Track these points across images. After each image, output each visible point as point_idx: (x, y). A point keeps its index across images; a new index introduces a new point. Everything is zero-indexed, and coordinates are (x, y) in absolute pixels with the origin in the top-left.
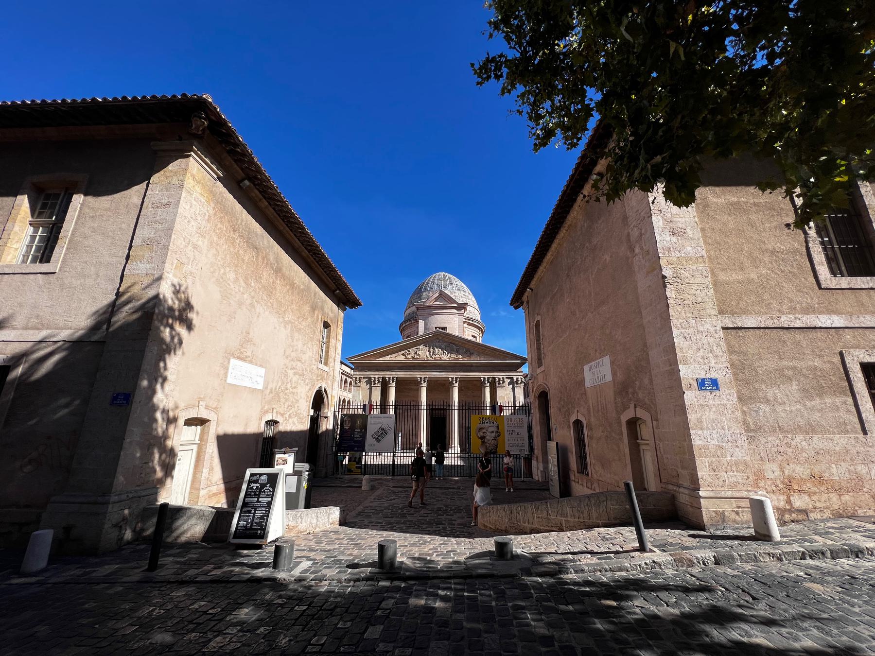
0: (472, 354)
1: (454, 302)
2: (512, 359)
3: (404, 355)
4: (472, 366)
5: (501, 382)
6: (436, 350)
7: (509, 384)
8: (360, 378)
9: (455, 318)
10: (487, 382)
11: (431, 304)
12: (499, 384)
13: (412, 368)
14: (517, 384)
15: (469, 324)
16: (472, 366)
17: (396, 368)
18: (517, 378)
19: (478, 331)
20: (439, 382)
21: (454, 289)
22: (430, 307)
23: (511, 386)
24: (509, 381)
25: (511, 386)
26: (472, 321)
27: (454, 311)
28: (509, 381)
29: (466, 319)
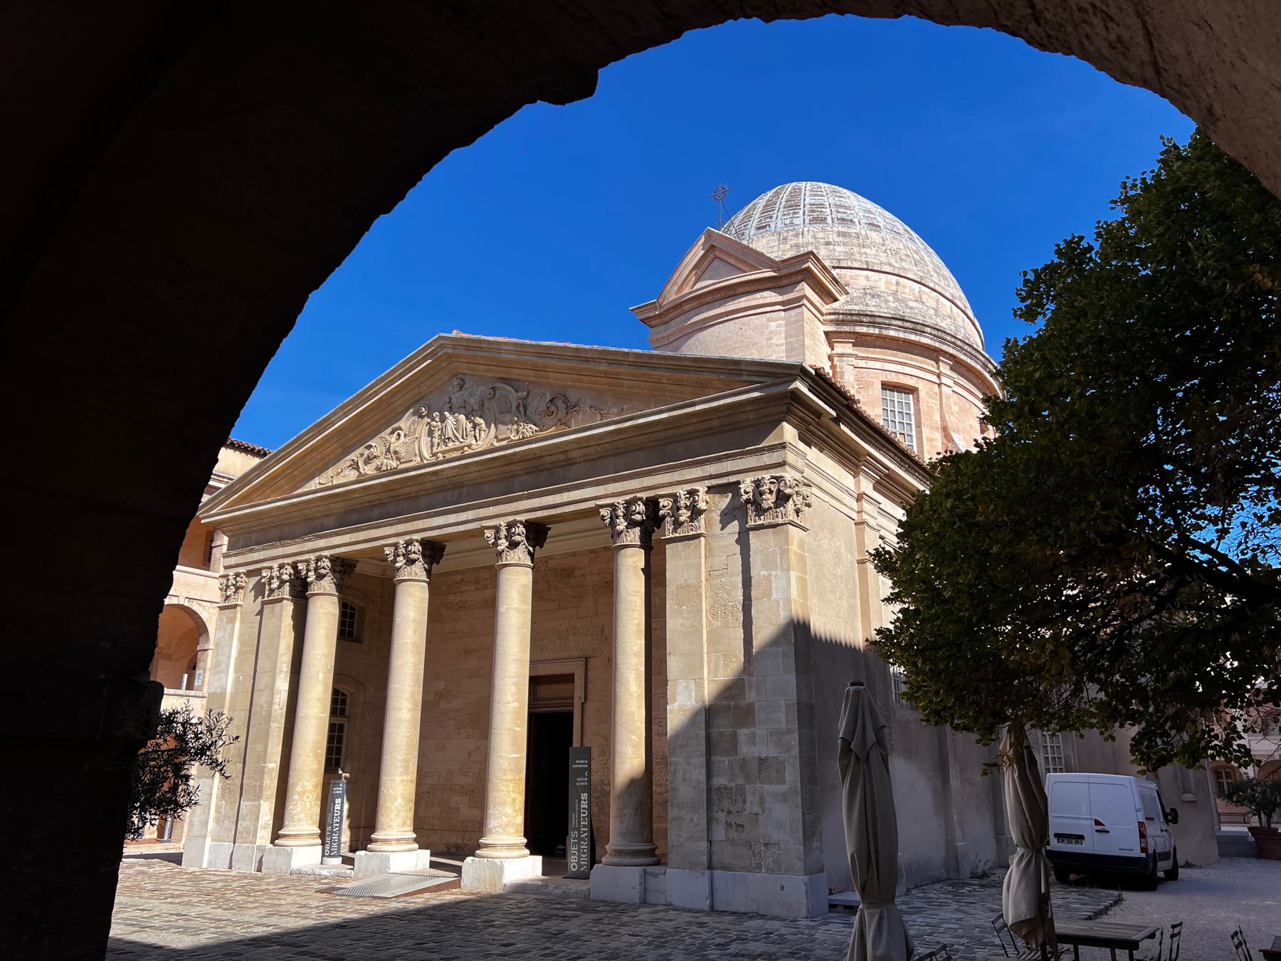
0: (571, 408)
1: (761, 260)
2: (702, 388)
3: (355, 466)
4: (570, 463)
5: (684, 515)
6: (451, 420)
7: (726, 517)
8: (237, 575)
9: (773, 325)
10: (622, 524)
11: (687, 290)
12: (677, 524)
13: (376, 512)
14: (760, 511)
15: (861, 341)
16: (570, 463)
17: (331, 521)
18: (758, 483)
19: (929, 364)
20: (551, 564)
21: (798, 221)
22: (680, 307)
23: (734, 526)
24: (724, 501)
25: (734, 526)
26: (873, 324)
27: (770, 296)
28: (724, 501)
29: (837, 322)
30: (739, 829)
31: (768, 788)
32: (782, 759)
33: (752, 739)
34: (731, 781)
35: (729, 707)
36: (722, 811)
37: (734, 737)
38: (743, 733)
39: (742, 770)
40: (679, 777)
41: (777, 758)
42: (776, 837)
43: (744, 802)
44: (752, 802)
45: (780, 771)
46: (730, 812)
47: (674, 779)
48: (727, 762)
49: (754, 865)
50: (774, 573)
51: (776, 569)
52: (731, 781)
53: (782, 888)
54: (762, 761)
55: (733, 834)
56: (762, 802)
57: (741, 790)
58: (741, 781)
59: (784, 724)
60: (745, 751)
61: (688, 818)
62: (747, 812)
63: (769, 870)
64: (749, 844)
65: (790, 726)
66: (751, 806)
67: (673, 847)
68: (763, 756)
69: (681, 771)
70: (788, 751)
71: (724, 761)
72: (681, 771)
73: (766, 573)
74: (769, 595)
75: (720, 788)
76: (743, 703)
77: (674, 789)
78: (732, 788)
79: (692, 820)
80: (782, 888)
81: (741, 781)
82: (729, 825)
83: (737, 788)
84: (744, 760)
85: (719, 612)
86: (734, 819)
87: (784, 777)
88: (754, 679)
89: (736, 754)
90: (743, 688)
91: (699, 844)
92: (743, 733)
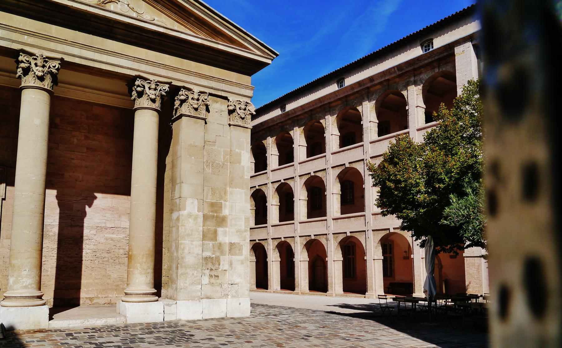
30: (217, 278)
31: (234, 258)
32: (242, 244)
33: (225, 233)
34: (213, 254)
35: (214, 216)
36: (208, 269)
37: (215, 232)
38: (220, 230)
39: (219, 249)
40: (186, 251)
41: (239, 243)
42: (237, 280)
43: (219, 265)
44: (223, 264)
45: (240, 249)
46: (211, 270)
47: (183, 253)
48: (211, 244)
49: (223, 295)
50: (243, 152)
51: (244, 150)
52: (213, 254)
53: (240, 304)
54: (231, 244)
55: (213, 280)
56: (231, 264)
57: (218, 260)
58: (218, 254)
59: (244, 227)
60: (221, 239)
61: (191, 273)
62: (220, 269)
63: (233, 297)
64: (221, 285)
65: (246, 229)
66: (224, 265)
67: (181, 289)
68: (233, 242)
69: (187, 249)
70: (245, 240)
71: (210, 244)
72: (187, 249)
73: (239, 151)
74: (240, 163)
75: (206, 257)
76: (221, 215)
77: (183, 258)
78: (213, 257)
79: (193, 274)
80: (240, 304)
81: (218, 254)
82: (211, 276)
83: (215, 258)
84: (220, 244)
85: (210, 165)
86: (213, 273)
87: (242, 252)
88: (227, 203)
89: (216, 240)
90: (221, 207)
91: (197, 286)
92: (220, 230)
